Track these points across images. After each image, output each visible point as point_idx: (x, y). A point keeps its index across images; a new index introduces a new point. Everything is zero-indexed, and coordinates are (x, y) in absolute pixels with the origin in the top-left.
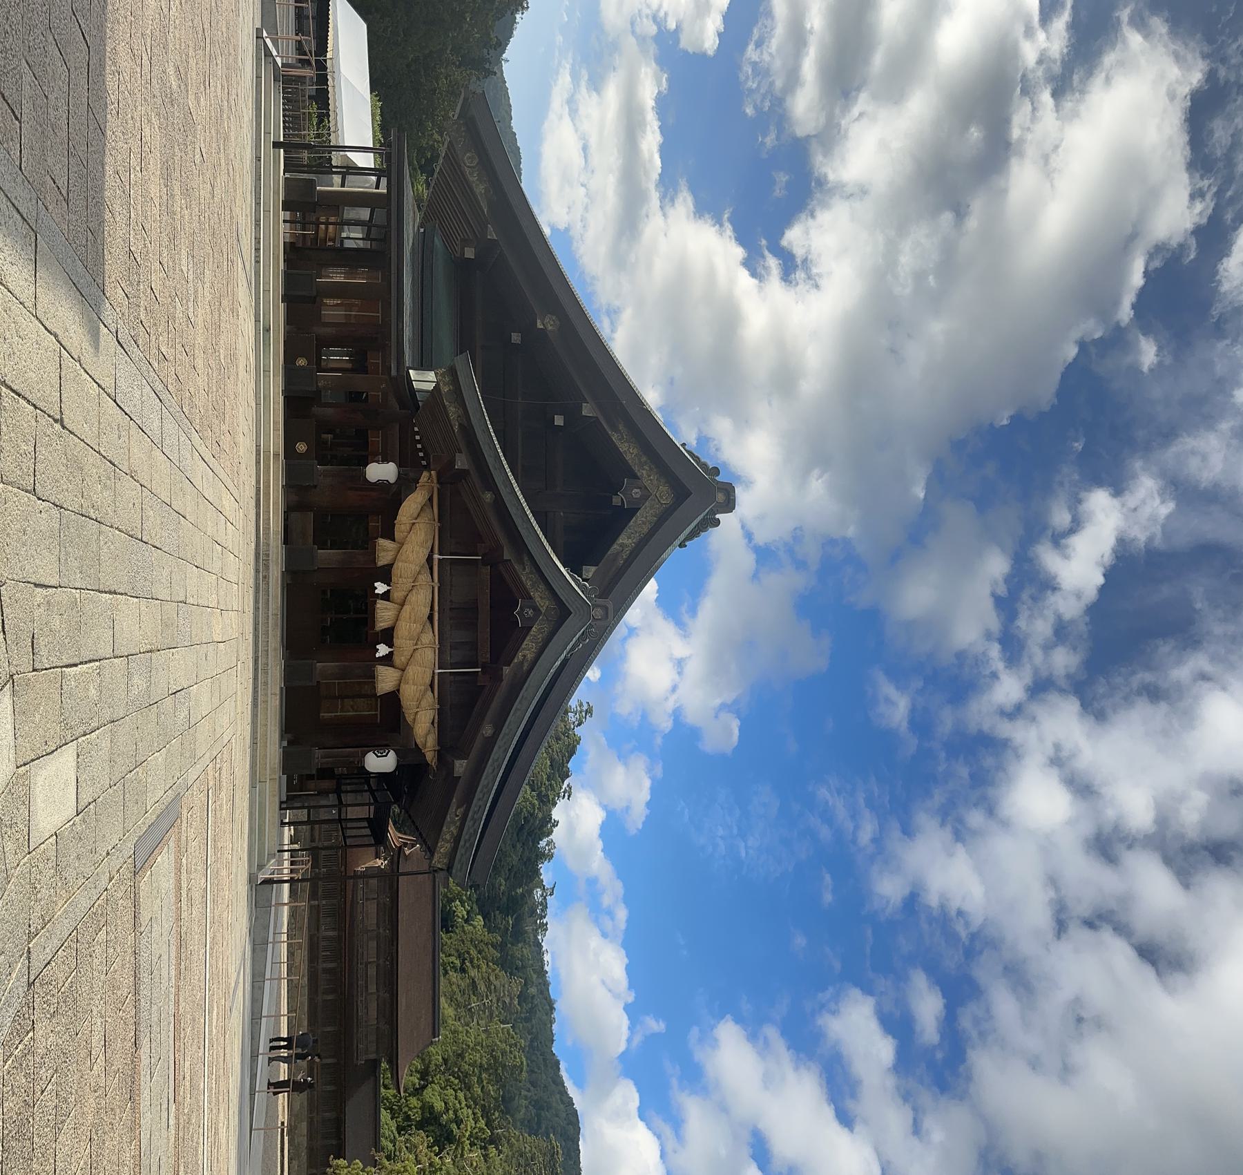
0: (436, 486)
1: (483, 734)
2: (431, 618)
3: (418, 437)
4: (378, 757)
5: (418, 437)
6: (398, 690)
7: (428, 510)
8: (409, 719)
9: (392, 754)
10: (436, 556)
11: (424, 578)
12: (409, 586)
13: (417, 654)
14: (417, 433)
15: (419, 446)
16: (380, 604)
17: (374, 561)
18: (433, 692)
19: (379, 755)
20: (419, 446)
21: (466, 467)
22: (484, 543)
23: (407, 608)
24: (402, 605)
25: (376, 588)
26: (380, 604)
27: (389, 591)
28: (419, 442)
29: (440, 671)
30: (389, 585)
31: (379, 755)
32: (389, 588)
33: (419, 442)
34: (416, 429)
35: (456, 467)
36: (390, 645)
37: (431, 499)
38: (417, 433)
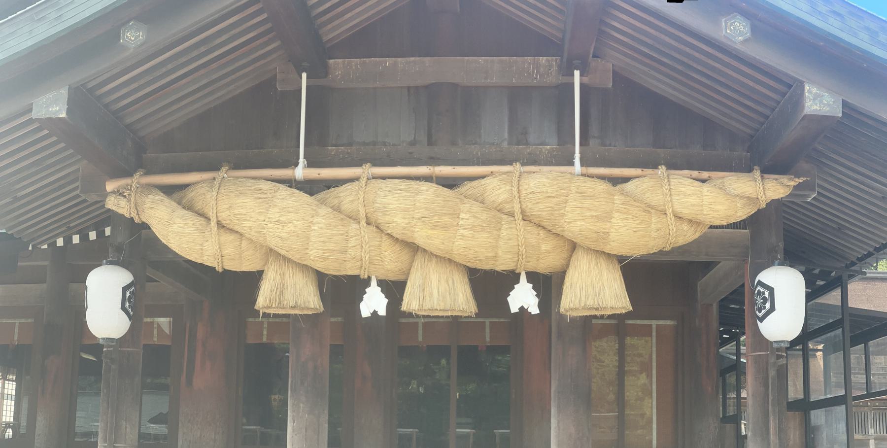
0: (139, 179)
1: (746, 41)
2: (450, 183)
3: (76, 239)
4: (772, 309)
5: (76, 239)
6: (621, 259)
7: (191, 194)
8: (686, 235)
9: (768, 276)
10: (300, 172)
11: (346, 196)
12: (367, 233)
13: (537, 209)
14: (68, 240)
15: (93, 235)
16: (411, 302)
17: (313, 319)
18: (626, 180)
19: (768, 306)
20: (93, 235)
21: (64, 92)
22: (274, 78)
23: (421, 236)
24: (414, 249)
25: (375, 313)
26: (411, 302)
27: (381, 283)
28: (84, 237)
29: (577, 161)
30: (367, 283)
31: (768, 306)
32: (374, 283)
33: (84, 237)
34: (60, 242)
35: (63, 115)
36: (511, 279)
37: (169, 190)
38: (68, 240)
